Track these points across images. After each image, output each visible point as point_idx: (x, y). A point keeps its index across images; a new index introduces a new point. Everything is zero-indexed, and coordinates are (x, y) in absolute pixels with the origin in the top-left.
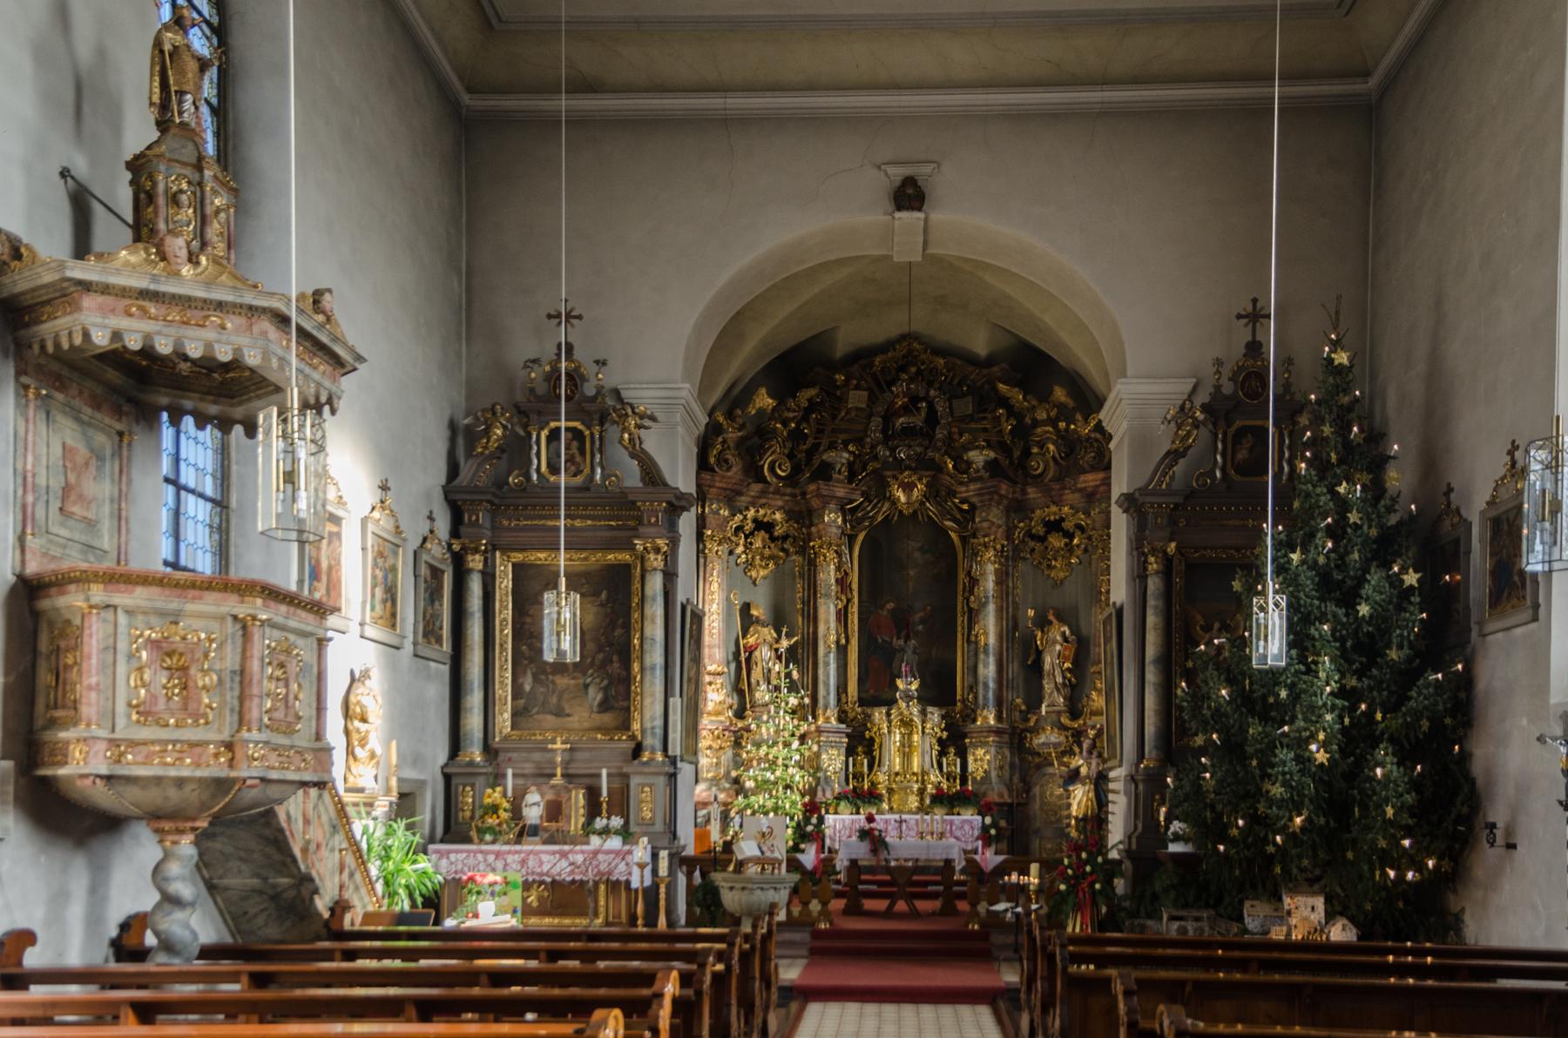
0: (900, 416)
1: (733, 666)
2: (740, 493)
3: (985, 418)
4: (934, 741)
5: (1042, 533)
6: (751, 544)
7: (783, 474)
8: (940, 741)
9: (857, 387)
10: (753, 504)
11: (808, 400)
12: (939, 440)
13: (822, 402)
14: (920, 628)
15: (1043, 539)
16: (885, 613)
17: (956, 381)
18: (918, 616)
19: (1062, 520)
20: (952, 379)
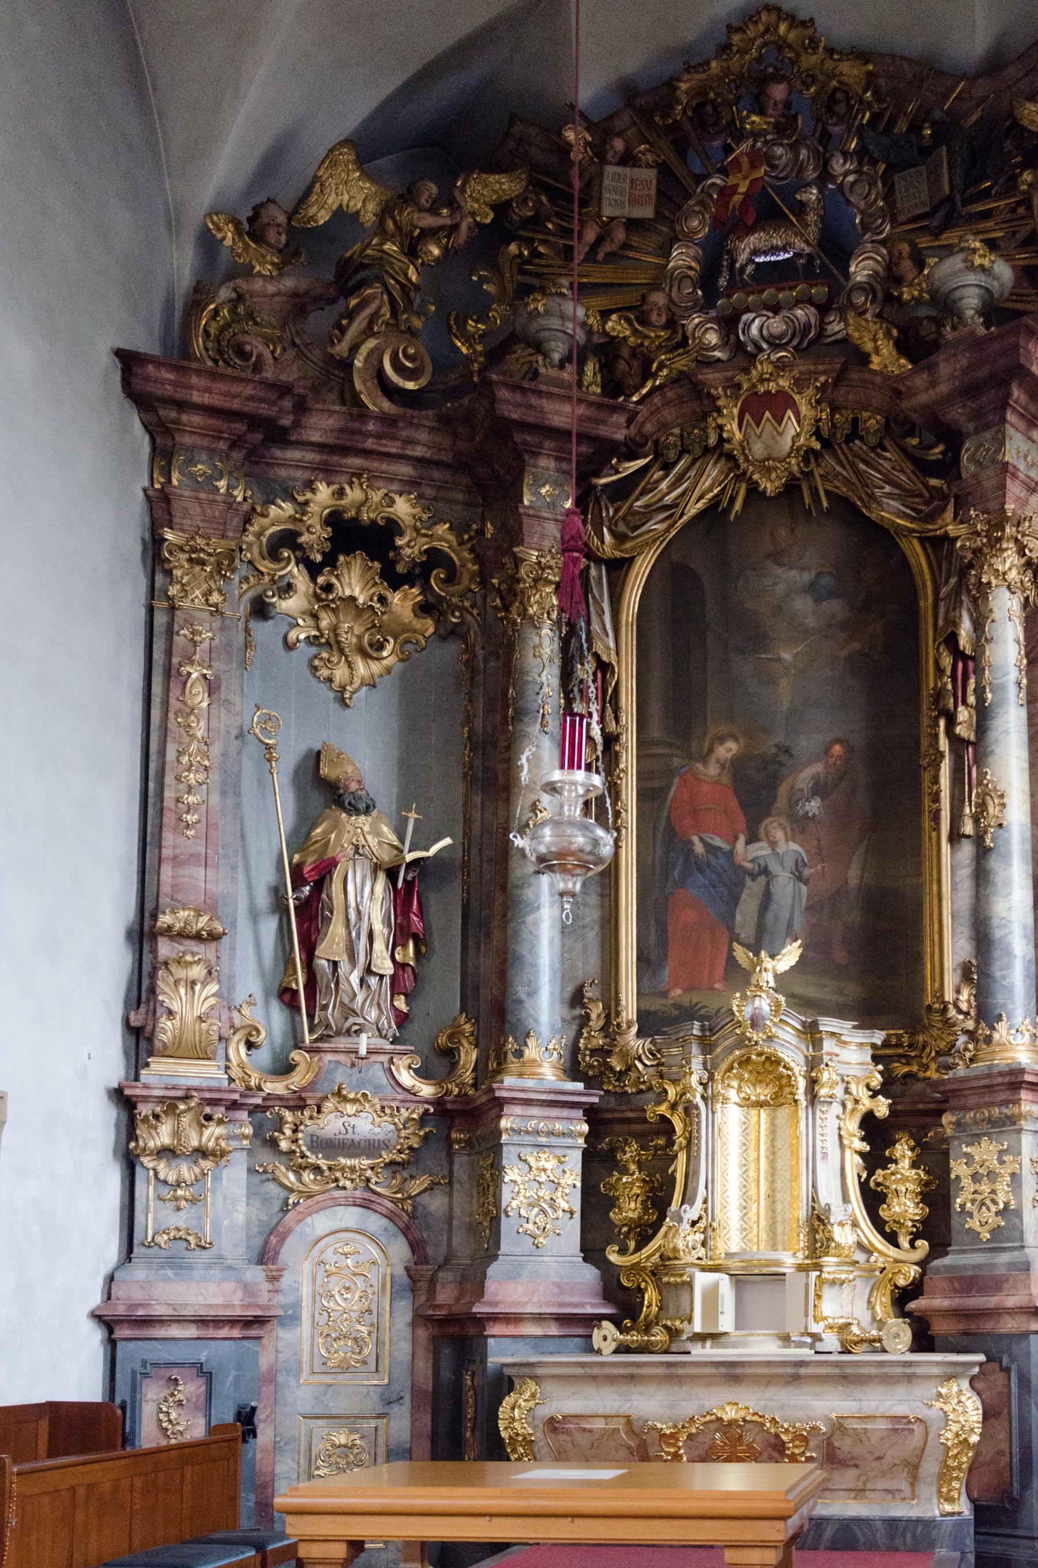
0: (750, 231)
2: (279, 436)
3: (986, 215)
4: (852, 1125)
7: (410, 385)
8: (869, 1122)
9: (628, 159)
11: (497, 207)
12: (860, 287)
13: (535, 222)
14: (814, 806)
16: (713, 770)
20: (893, 120)
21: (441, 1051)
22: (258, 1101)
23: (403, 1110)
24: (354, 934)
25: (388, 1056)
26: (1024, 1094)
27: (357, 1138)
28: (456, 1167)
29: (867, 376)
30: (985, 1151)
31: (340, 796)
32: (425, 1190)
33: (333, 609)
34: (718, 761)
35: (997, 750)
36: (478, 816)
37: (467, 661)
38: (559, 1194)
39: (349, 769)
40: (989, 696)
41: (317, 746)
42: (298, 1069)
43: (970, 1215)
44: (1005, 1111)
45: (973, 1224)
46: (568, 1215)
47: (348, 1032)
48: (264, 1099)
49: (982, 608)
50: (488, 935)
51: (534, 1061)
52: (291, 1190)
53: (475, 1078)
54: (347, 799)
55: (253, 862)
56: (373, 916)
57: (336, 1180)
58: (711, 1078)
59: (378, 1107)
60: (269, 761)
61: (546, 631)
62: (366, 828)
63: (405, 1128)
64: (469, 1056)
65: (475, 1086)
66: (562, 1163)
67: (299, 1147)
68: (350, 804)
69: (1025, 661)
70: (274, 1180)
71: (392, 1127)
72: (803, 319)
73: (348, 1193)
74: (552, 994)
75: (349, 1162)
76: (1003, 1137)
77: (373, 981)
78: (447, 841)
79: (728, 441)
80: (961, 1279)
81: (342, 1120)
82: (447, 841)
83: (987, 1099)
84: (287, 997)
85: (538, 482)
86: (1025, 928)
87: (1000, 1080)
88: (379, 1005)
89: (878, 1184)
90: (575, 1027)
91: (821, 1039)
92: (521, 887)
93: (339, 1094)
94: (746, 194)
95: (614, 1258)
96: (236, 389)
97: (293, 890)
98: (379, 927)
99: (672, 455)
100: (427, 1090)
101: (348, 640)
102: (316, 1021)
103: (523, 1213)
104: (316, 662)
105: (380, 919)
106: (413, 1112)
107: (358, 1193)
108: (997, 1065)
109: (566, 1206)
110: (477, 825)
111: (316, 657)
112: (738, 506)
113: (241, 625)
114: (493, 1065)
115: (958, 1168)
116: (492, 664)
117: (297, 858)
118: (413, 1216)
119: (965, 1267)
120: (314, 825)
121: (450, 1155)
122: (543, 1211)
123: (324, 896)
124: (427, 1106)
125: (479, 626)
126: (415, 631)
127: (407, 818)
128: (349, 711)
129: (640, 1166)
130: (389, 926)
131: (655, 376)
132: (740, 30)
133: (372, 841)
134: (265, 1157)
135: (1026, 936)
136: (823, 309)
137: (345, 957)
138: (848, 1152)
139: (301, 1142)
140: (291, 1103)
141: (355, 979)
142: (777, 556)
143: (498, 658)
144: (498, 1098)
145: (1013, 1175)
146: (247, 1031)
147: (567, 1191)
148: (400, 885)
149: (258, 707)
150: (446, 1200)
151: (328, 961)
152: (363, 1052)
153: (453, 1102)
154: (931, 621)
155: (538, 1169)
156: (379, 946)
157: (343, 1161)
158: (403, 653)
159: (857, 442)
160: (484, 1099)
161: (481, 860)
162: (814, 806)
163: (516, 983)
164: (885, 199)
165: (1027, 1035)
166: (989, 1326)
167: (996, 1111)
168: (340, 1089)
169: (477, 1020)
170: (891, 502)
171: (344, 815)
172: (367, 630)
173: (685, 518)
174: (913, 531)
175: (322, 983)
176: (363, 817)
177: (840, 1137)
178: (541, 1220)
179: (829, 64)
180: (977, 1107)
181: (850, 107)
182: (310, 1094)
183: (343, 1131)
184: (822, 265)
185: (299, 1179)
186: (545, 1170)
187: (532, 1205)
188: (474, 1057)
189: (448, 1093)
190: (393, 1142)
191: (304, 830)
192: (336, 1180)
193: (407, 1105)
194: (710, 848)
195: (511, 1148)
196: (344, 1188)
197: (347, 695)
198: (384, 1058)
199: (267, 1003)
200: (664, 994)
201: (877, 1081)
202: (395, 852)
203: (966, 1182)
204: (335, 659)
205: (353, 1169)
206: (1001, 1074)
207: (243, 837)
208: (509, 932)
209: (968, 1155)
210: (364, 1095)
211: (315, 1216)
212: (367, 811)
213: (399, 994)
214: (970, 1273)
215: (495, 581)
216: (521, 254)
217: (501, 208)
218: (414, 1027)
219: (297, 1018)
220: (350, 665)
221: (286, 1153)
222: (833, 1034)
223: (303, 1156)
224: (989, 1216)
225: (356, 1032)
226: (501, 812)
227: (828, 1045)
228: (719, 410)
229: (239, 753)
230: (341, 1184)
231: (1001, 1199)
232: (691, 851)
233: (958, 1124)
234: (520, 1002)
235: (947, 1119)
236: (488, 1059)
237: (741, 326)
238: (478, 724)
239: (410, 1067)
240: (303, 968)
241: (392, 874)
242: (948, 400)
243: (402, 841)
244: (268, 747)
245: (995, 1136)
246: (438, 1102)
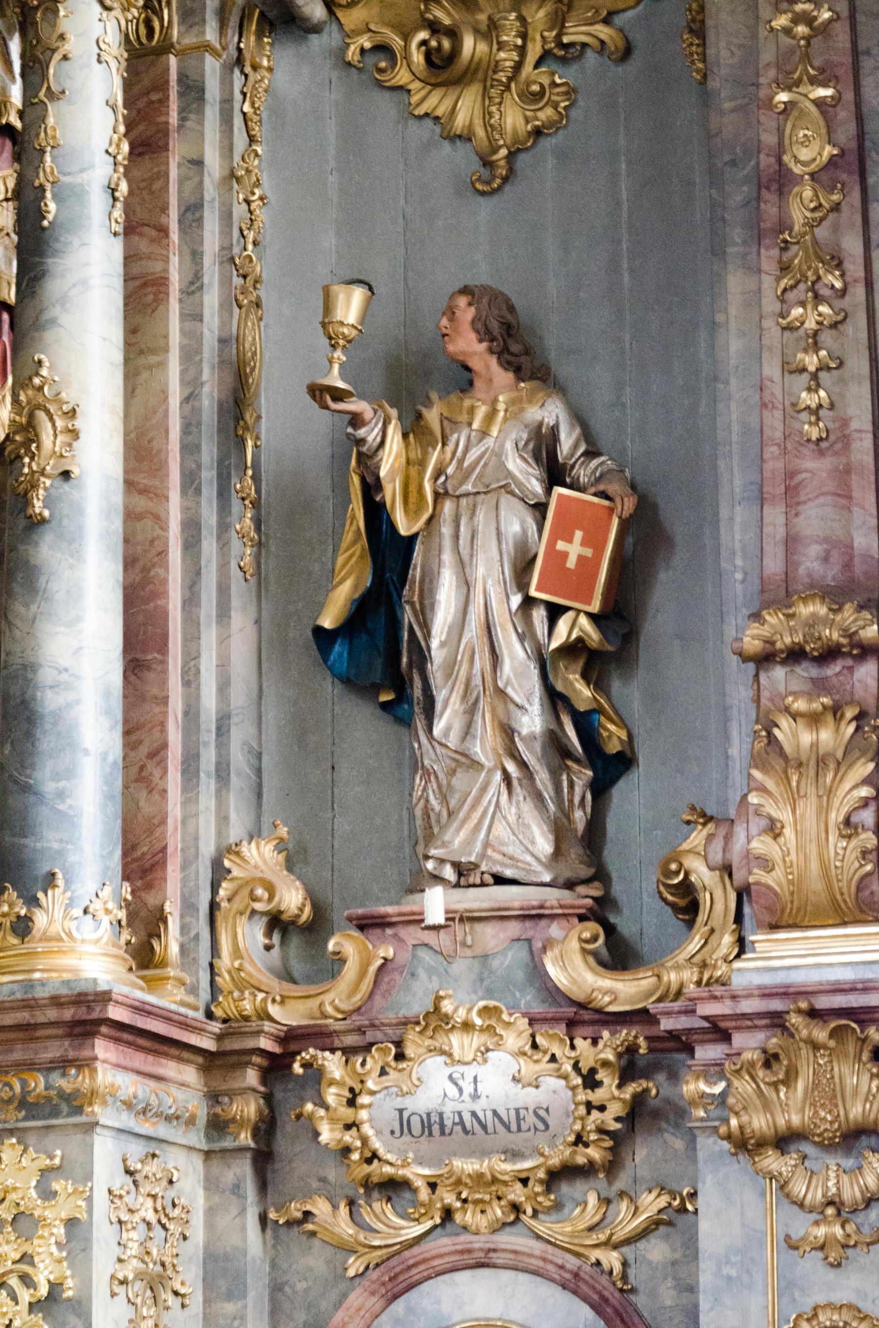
26: (102, 1049)
44: (59, 1081)
76: (51, 1139)
83: (18, 1055)
86: (107, 694)
108: (43, 983)
135: (108, 712)
145: (71, 1223)
165: (106, 920)
167: (38, 1083)
231: (43, 1276)
245: (32, 1139)
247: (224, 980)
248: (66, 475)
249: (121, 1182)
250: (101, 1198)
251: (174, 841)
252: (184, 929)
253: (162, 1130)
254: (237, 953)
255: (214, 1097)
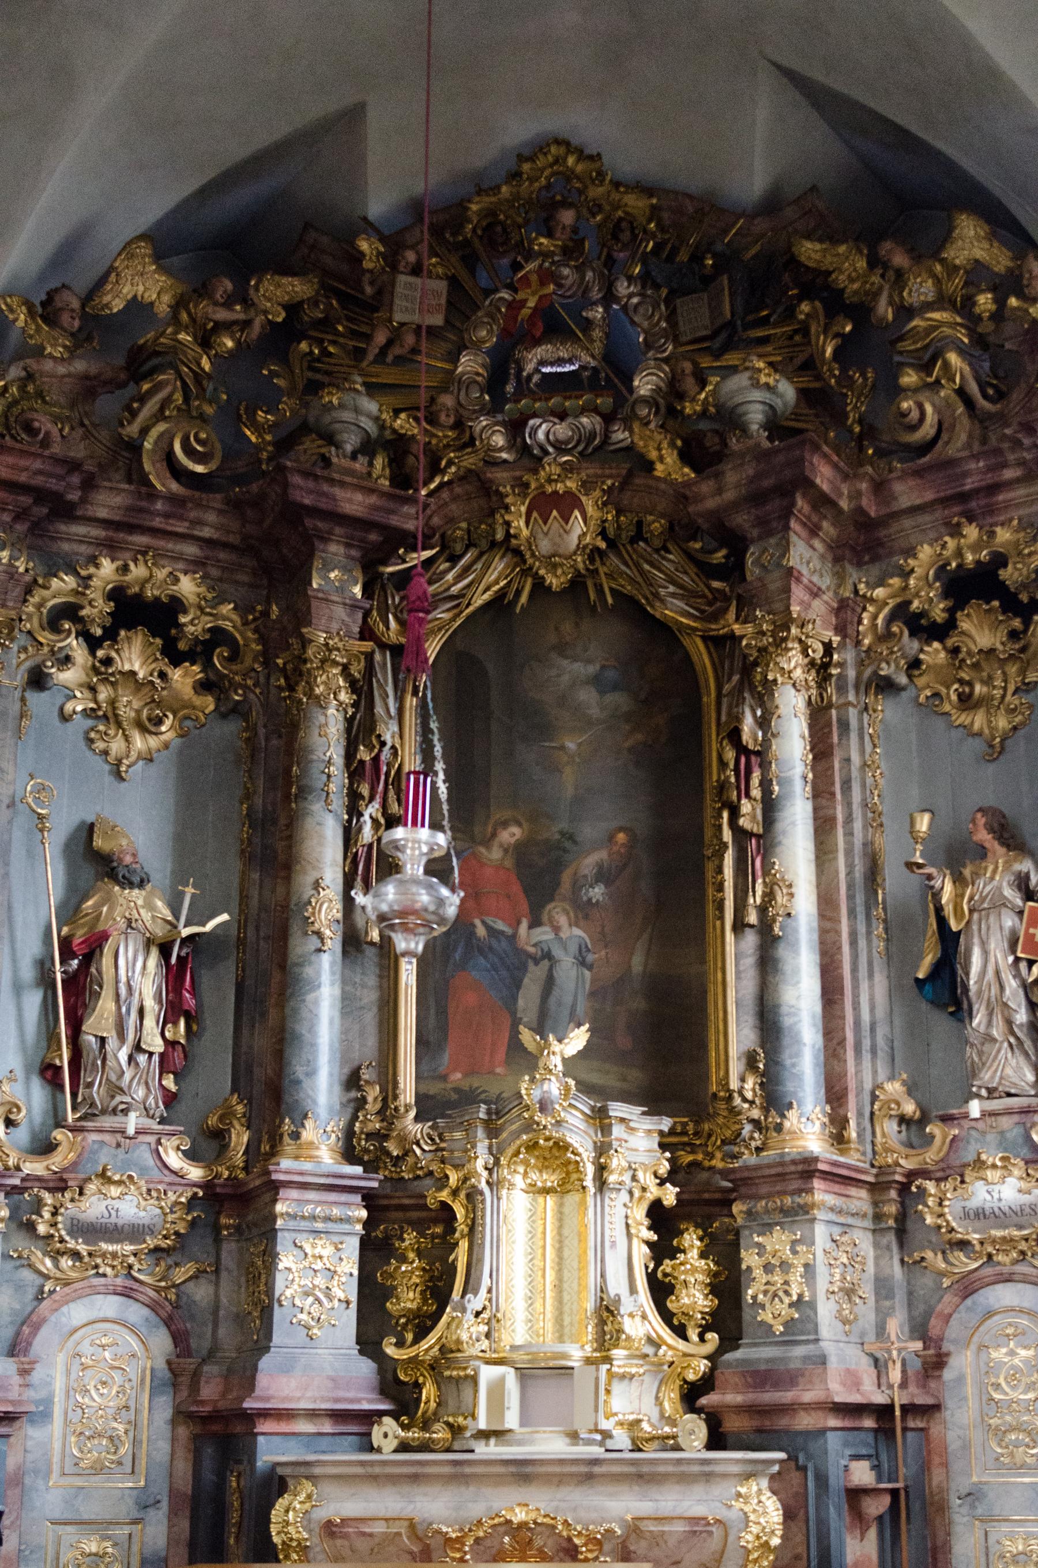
0: (537, 342)
1: (34, 1000)
4: (639, 1213)
5: (938, 613)
6: (108, 661)
8: (656, 1212)
10: (112, 548)
12: (644, 400)
14: (597, 892)
15: (939, 632)
17: (683, 256)
18: (589, 863)
19: (1000, 560)
21: (211, 1132)
22: (17, 1182)
23: (170, 1194)
24: (124, 1009)
25: (156, 1137)
26: (817, 1183)
27: (120, 1222)
28: (224, 1255)
29: (651, 482)
30: (778, 1241)
31: (113, 869)
32: (190, 1278)
33: (112, 684)
34: (501, 845)
35: (785, 841)
36: (255, 893)
37: (248, 739)
38: (335, 1283)
39: (124, 842)
40: (776, 788)
41: (90, 818)
42: (60, 1149)
43: (763, 1307)
44: (798, 1200)
45: (765, 1316)
46: (344, 1305)
47: (114, 1112)
48: (23, 1180)
49: (768, 705)
50: (263, 1015)
51: (312, 1143)
52: (47, 1277)
53: (246, 1162)
54: (121, 872)
55: (19, 934)
56: (145, 991)
57: (97, 1267)
58: (497, 1162)
59: (144, 1189)
60: (42, 831)
61: (332, 711)
62: (140, 902)
63: (172, 1212)
64: (240, 1138)
65: (246, 1169)
66: (338, 1250)
67: (58, 1230)
68: (124, 877)
69: (810, 757)
70: (29, 1266)
71: (158, 1211)
72: (589, 427)
73: (109, 1281)
74: (331, 1075)
75: (111, 1247)
76: (795, 1226)
77: (142, 1059)
78: (225, 917)
79: (515, 537)
80: (755, 1373)
81: (105, 1203)
82: (225, 917)
83: (778, 1188)
84: (49, 1074)
85: (327, 568)
86: (814, 1017)
87: (793, 1168)
88: (147, 1083)
89: (666, 1275)
90: (350, 1111)
91: (611, 1125)
92: (301, 965)
93: (103, 1175)
94: (535, 309)
95: (390, 1351)
96: (23, 462)
97: (61, 963)
98: (150, 1003)
99: (458, 548)
100: (195, 1173)
101: (126, 713)
102: (79, 1100)
103: (298, 1302)
104: (93, 735)
105: (151, 994)
106: (179, 1196)
107: (119, 1281)
108: (789, 1154)
109: (342, 1296)
110: (254, 902)
111: (92, 729)
112: (524, 599)
113: (17, 694)
114: (265, 1147)
115: (750, 1259)
116: (275, 742)
117: (65, 930)
118: (176, 1306)
119: (758, 1360)
120: (85, 898)
121: (218, 1240)
122: (318, 1299)
123: (93, 970)
124: (195, 1189)
125: (262, 705)
126: (194, 708)
127: (182, 894)
128: (124, 785)
129: (419, 1254)
130: (160, 1002)
131: (443, 472)
132: (531, 159)
133: (146, 915)
134: (21, 1242)
135: (815, 1025)
136: (608, 419)
137: (114, 1034)
138: (635, 1241)
139: (60, 1226)
140: (51, 1185)
141: (123, 1055)
142: (562, 649)
143: (280, 736)
144: (273, 1181)
145: (806, 1266)
146: (7, 1108)
147: (343, 1279)
148: (173, 960)
149: (32, 777)
150: (211, 1290)
151: (96, 1036)
152: (131, 1131)
153: (223, 1186)
154: (713, 715)
155: (314, 1256)
156: (149, 1022)
157: (104, 1246)
158: (181, 728)
159: (641, 544)
160: (258, 1182)
161: (258, 939)
162: (597, 892)
163: (294, 1062)
164: (668, 320)
165: (818, 1123)
166: (783, 1422)
167: (788, 1200)
168: (104, 1170)
169: (250, 1103)
170: (675, 601)
171: (117, 888)
172: (147, 704)
173: (471, 609)
174: (695, 629)
175: (86, 1060)
176: (136, 891)
177: (627, 1225)
178: (315, 1310)
179: (615, 196)
180: (769, 1196)
181: (635, 237)
182: (72, 1175)
183: (106, 1214)
184: (608, 379)
185: (57, 1266)
186: (321, 1257)
187: (307, 1294)
188: (245, 1139)
189: (218, 1176)
190: (159, 1227)
191: (74, 901)
192: (97, 1267)
193: (174, 1188)
194: (490, 930)
195: (286, 1234)
196: (104, 1275)
197: (123, 768)
198: (152, 1139)
199: (28, 1079)
200: (444, 1078)
201: (664, 1168)
202: (169, 927)
203: (757, 1273)
204: (111, 732)
205: (114, 1255)
206: (794, 1162)
207: (10, 908)
208: (287, 1011)
209: (759, 1245)
210: (130, 1177)
211: (72, 1305)
212: (141, 885)
213: (168, 1072)
214: (763, 1367)
215: (280, 661)
216: (311, 352)
217: (293, 309)
218: (182, 1107)
219: (59, 1095)
220: (127, 738)
221: (44, 1237)
222: (622, 1120)
223: (62, 1241)
224: (782, 1308)
225: (122, 1111)
226: (280, 890)
227: (618, 1131)
228: (507, 508)
229: (10, 822)
230: (101, 1271)
231: (795, 1291)
232: (473, 933)
233: (749, 1213)
234: (298, 1082)
235: (737, 1208)
236: (260, 1142)
237: (527, 430)
238: (258, 801)
239: (178, 1149)
240: (68, 1044)
241: (165, 950)
242: (735, 506)
243: (177, 916)
244: (41, 817)
245: (786, 1226)
246: (207, 1186)
247: (879, 1148)
248: (789, 915)
249: (829, 1245)
250: (820, 1254)
251: (852, 1084)
252: (858, 1124)
253: (850, 1221)
254: (884, 1135)
255: (875, 1204)
